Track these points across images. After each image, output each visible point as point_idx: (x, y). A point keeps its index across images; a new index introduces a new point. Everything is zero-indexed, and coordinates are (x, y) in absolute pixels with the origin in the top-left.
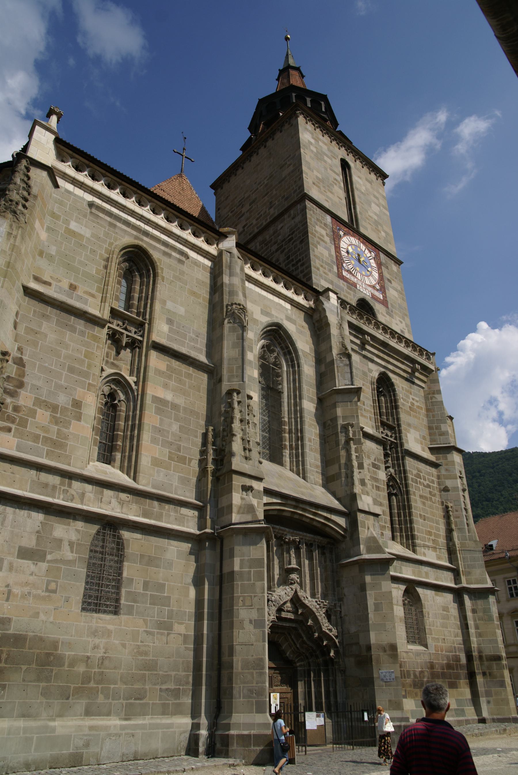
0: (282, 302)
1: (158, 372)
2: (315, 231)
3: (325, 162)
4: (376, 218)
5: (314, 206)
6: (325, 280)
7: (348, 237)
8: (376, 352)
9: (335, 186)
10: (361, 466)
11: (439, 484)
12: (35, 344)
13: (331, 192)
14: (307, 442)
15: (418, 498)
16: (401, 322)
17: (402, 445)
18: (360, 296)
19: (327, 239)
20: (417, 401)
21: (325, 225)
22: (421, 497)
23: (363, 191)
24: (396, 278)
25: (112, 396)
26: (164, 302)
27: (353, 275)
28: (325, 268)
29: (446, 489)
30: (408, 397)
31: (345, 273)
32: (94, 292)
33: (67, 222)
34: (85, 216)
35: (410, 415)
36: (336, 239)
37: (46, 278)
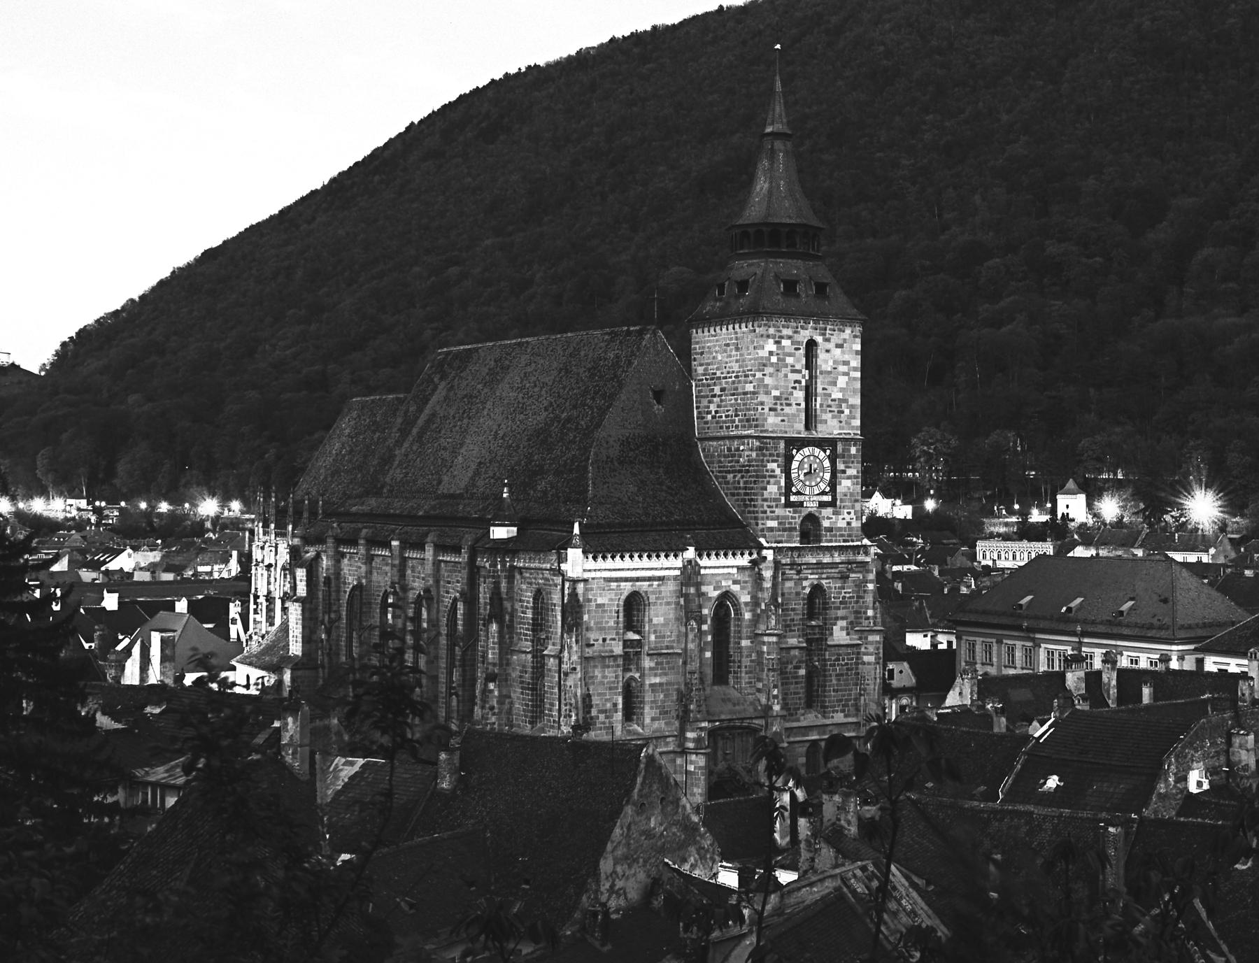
0: (730, 570)
1: (651, 669)
2: (767, 471)
3: (786, 366)
4: (840, 396)
5: (768, 441)
6: (772, 520)
7: (801, 452)
8: (810, 571)
9: (795, 391)
11: (857, 659)
12: (593, 683)
13: (789, 405)
14: (743, 669)
15: (833, 678)
16: (849, 513)
17: (826, 640)
18: (805, 512)
19: (778, 471)
20: (849, 593)
21: (778, 455)
22: (836, 675)
23: (829, 369)
24: (853, 462)
26: (650, 621)
27: (801, 494)
28: (772, 507)
29: (864, 663)
30: (840, 593)
31: (793, 498)
32: (614, 637)
33: (596, 600)
34: (604, 590)
35: (838, 608)
36: (789, 459)
37: (592, 642)
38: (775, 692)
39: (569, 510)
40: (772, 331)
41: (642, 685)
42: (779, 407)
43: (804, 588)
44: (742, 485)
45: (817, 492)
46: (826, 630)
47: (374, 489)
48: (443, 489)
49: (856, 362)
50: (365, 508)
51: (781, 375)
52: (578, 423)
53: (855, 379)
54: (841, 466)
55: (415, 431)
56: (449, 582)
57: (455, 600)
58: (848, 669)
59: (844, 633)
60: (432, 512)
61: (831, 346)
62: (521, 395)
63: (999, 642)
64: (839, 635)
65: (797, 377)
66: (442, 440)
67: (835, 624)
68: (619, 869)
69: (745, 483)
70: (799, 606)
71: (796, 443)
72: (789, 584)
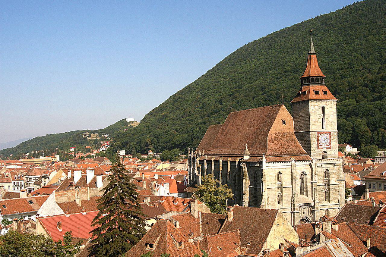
1: (284, 191)
4: (331, 120)
7: (321, 135)
9: (319, 119)
10: (316, 195)
13: (317, 123)
15: (332, 193)
16: (335, 150)
18: (323, 150)
19: (315, 140)
23: (328, 113)
25: (279, 195)
29: (339, 189)
30: (333, 171)
31: (320, 147)
36: (318, 137)
38: (317, 197)
39: (262, 152)
40: (312, 104)
41: (282, 195)
42: (315, 124)
43: (323, 170)
44: (306, 144)
45: (326, 145)
46: (329, 180)
47: (216, 147)
48: (232, 147)
49: (335, 111)
50: (214, 153)
51: (315, 115)
52: (264, 130)
53: (335, 115)
54: (332, 138)
55: (225, 133)
56: (234, 170)
57: (235, 174)
58: (336, 191)
59: (335, 181)
60: (229, 153)
61: (328, 107)
62: (250, 123)
63: (377, 183)
64: (333, 182)
65: (320, 116)
66: (231, 135)
67: (332, 179)
68: (272, 240)
69: (307, 143)
70: (323, 175)
71: (319, 133)
72: (319, 169)
